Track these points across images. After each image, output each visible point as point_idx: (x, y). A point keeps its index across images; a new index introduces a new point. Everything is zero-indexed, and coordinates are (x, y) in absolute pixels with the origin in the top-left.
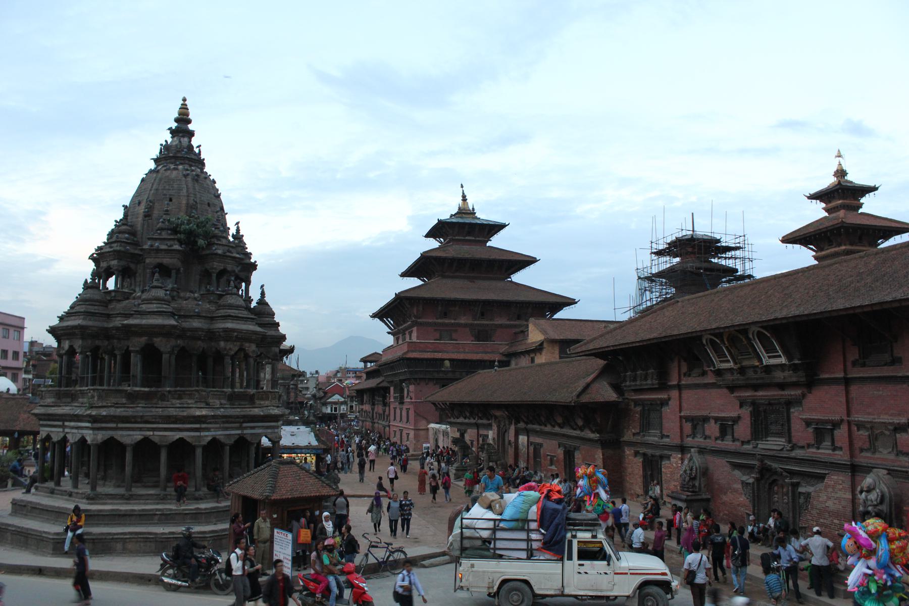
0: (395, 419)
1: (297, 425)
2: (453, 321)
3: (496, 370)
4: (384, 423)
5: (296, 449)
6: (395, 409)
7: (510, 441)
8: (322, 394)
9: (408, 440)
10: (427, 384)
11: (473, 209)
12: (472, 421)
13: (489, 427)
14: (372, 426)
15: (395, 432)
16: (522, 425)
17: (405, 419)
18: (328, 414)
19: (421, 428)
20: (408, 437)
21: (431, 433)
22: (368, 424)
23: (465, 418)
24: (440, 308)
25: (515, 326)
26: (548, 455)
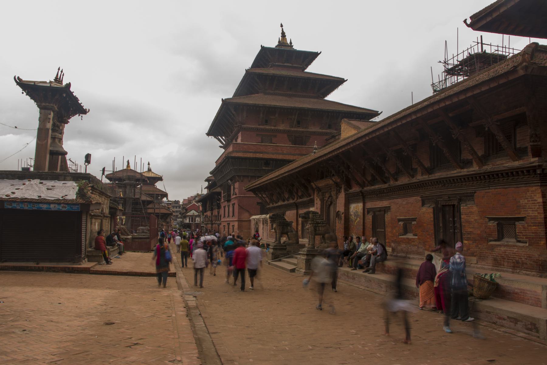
0: (224, 216)
1: (64, 180)
2: (273, 128)
3: (315, 153)
4: (218, 222)
5: (41, 203)
6: (225, 207)
7: (338, 214)
8: (185, 211)
9: (233, 232)
10: (249, 181)
11: (291, 43)
12: (291, 201)
13: (311, 203)
14: (212, 227)
15: (225, 226)
16: (356, 189)
17: (231, 214)
18: (187, 223)
19: (244, 220)
20: (233, 228)
21: (253, 223)
22: (210, 226)
23: (284, 201)
24: (262, 115)
25: (326, 134)
26: (400, 220)
